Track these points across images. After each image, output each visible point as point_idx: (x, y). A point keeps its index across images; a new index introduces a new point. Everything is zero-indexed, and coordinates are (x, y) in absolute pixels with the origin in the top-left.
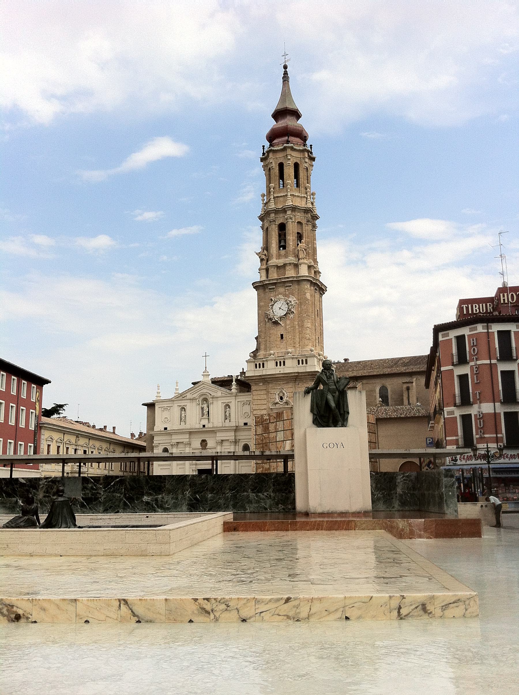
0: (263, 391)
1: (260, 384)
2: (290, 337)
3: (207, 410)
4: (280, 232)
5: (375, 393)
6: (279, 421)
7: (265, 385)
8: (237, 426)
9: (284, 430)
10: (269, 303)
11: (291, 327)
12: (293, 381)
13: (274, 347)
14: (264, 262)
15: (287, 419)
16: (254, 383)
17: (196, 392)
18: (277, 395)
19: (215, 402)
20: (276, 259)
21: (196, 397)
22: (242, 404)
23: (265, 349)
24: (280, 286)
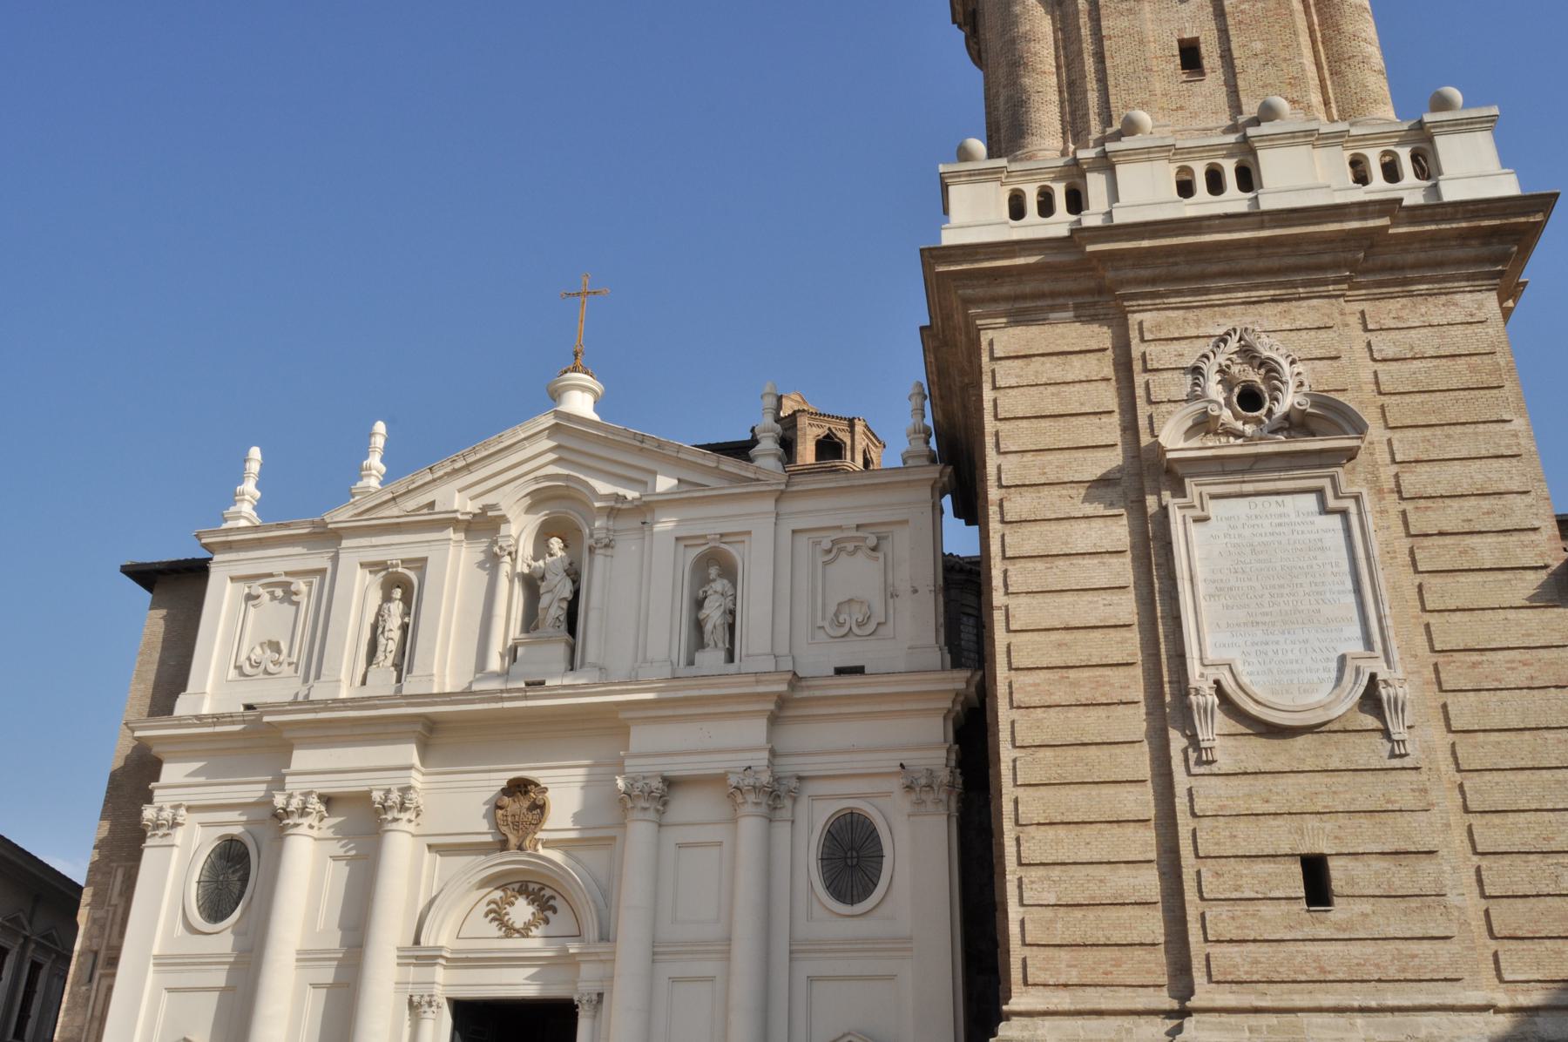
1: (1052, 316)
2: (1258, 46)
3: (567, 592)
19: (628, 547)
21: (493, 507)
22: (826, 544)
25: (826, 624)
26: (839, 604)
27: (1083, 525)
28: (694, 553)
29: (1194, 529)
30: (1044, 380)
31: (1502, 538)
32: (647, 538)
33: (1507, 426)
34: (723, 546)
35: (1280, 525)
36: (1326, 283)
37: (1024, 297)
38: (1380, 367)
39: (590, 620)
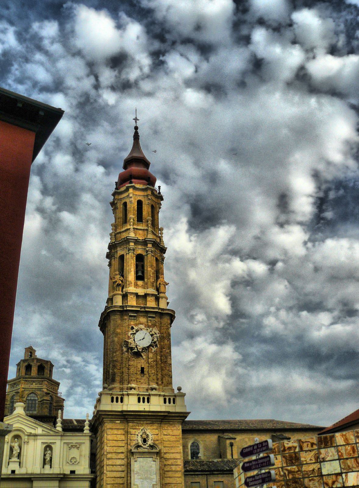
0: (120, 431)
1: (117, 422)
2: (153, 371)
3: (19, 451)
4: (137, 263)
5: (188, 449)
6: (323, 448)
7: (123, 423)
8: (64, 475)
9: (339, 459)
10: (128, 331)
11: (154, 361)
12: (159, 421)
13: (134, 380)
14: (120, 288)
15: (344, 444)
16: (109, 419)
17: (26, 424)
18: (139, 437)
19: (31, 442)
20: (134, 287)
22: (70, 446)
23: (122, 382)
24: (141, 316)
25: (69, 462)
26: (72, 458)
27: (118, 460)
28: (44, 446)
29: (135, 462)
30: (114, 433)
31: (176, 466)
32: (36, 442)
33: (179, 448)
34: (50, 444)
35: (146, 463)
36: (158, 421)
37: (113, 418)
38: (164, 436)
39: (23, 458)
